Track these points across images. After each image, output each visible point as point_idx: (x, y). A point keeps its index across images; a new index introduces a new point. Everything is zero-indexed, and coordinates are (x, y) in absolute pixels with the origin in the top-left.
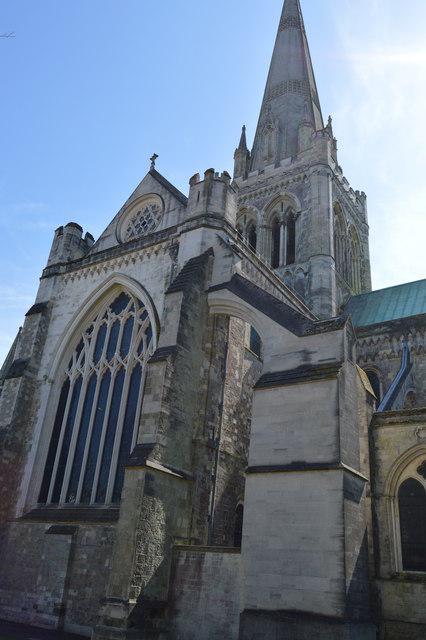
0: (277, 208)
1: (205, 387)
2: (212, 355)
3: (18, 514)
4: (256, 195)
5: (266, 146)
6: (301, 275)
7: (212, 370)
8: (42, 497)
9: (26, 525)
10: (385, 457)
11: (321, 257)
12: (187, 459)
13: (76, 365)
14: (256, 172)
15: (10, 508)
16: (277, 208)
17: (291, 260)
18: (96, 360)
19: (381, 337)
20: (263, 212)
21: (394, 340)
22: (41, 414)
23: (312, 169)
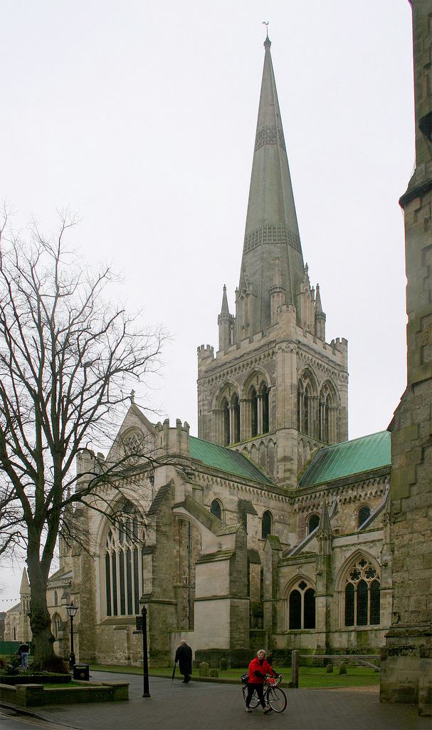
0: (254, 382)
1: (178, 560)
2: (180, 542)
3: (98, 622)
4: (236, 370)
5: (244, 313)
6: (271, 444)
7: (181, 550)
8: (109, 613)
9: (103, 627)
10: (283, 581)
11: (283, 431)
12: (172, 594)
13: (110, 545)
14: (234, 347)
15: (94, 619)
16: (254, 382)
17: (266, 430)
18: (121, 542)
19: (322, 493)
20: (242, 387)
21: (330, 495)
22: (97, 573)
23: (277, 347)
